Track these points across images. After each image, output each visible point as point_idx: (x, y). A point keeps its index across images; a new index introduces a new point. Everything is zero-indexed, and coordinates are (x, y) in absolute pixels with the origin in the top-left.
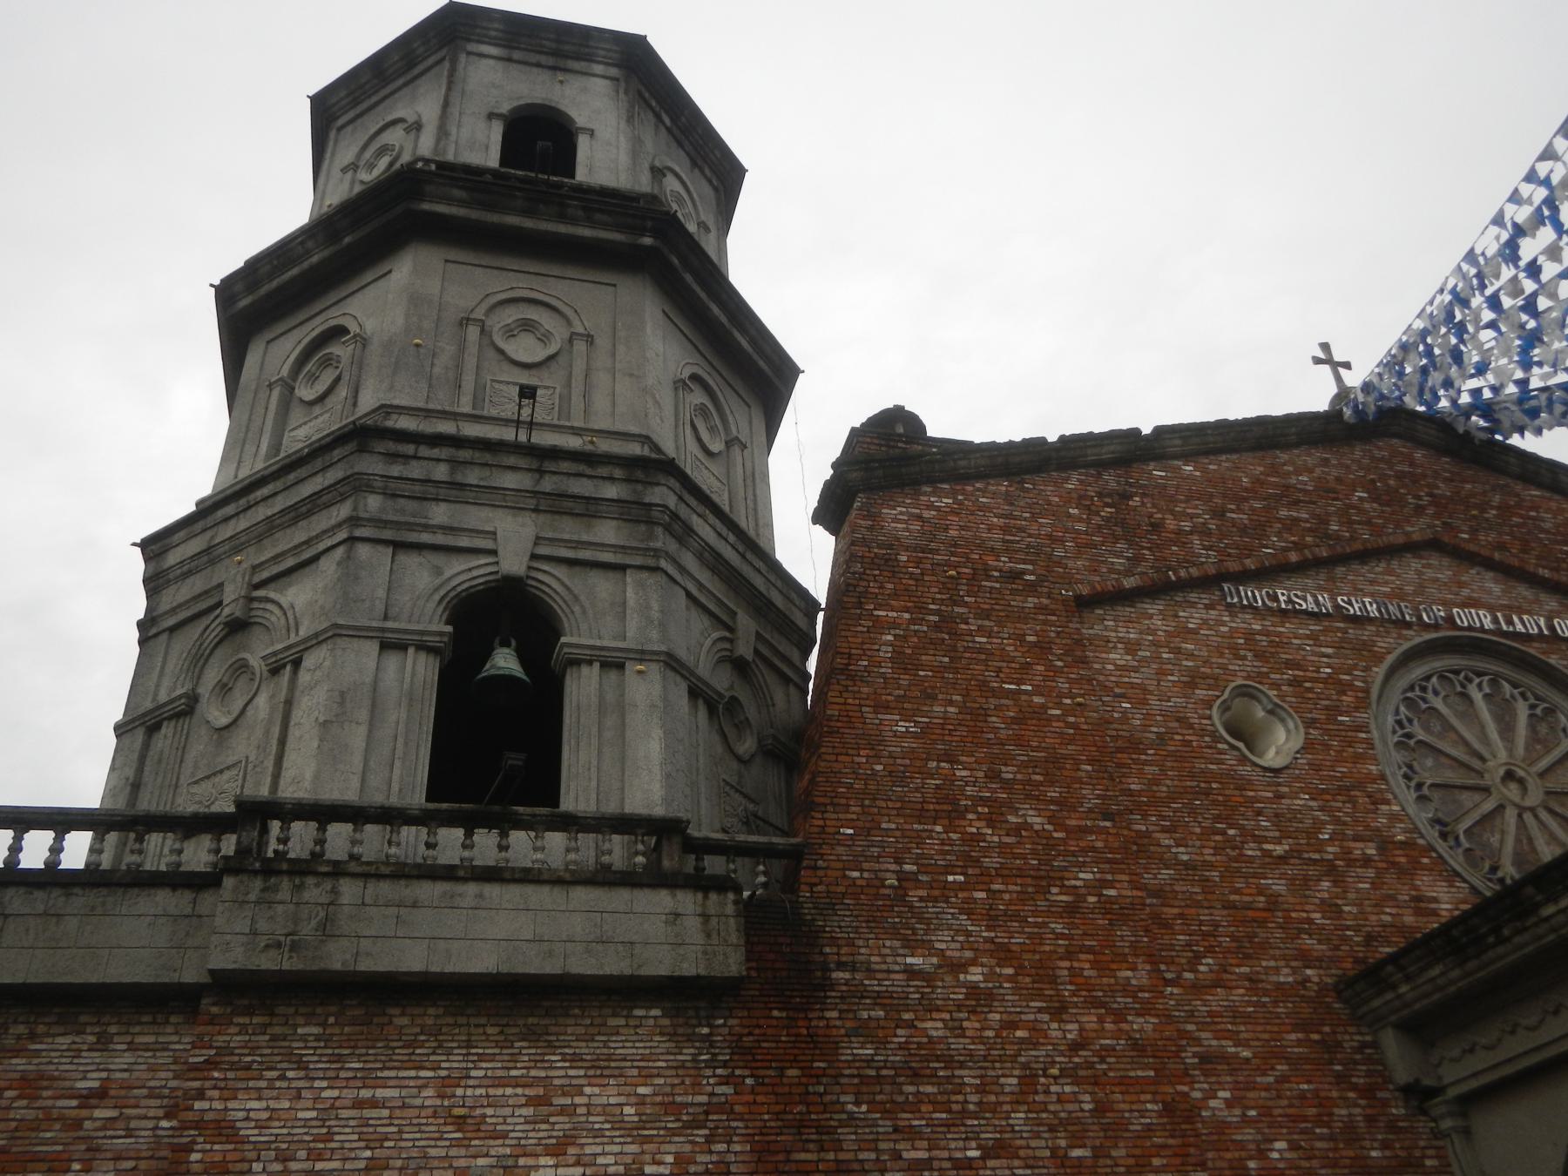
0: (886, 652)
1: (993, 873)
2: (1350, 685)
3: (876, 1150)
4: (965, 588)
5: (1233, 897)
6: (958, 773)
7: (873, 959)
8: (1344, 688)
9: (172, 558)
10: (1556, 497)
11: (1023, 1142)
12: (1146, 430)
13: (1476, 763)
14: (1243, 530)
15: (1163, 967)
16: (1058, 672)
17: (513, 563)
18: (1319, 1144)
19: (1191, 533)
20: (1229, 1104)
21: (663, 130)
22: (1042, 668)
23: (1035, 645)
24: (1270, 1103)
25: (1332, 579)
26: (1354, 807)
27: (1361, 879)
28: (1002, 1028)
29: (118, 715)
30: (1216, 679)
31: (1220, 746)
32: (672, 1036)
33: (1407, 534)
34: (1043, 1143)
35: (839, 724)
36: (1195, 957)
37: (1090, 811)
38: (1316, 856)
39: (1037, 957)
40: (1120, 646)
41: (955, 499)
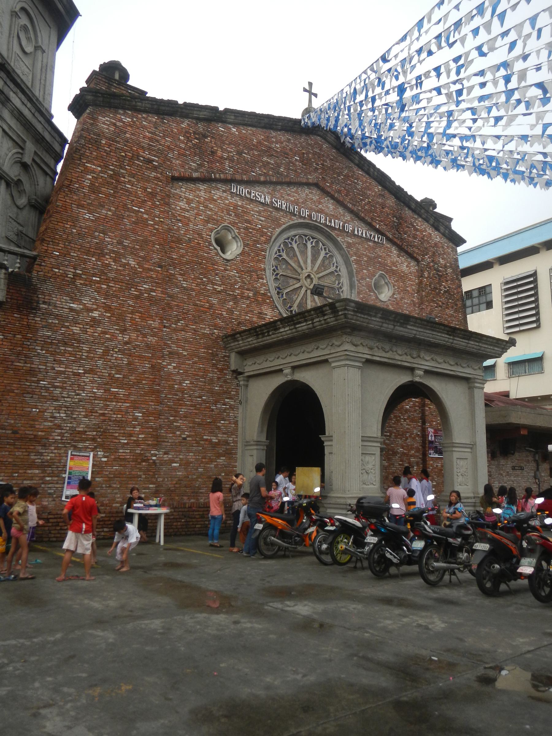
0: (87, 183)
1: (111, 279)
2: (266, 233)
3: (46, 366)
4: (127, 162)
5: (197, 302)
6: (106, 239)
7: (58, 302)
8: (263, 234)
10: (367, 176)
11: (100, 370)
12: (221, 109)
13: (299, 270)
14: (247, 163)
15: (165, 321)
16: (157, 206)
18: (200, 383)
19: (226, 159)
22: (150, 203)
23: (150, 193)
24: (188, 369)
25: (274, 190)
26: (251, 278)
27: (244, 303)
28: (101, 333)
30: (218, 221)
31: (211, 247)
33: (308, 179)
34: (106, 371)
35: (61, 210)
36: (178, 320)
37: (154, 263)
38: (232, 293)
39: (120, 311)
40: (185, 200)
41: (132, 119)
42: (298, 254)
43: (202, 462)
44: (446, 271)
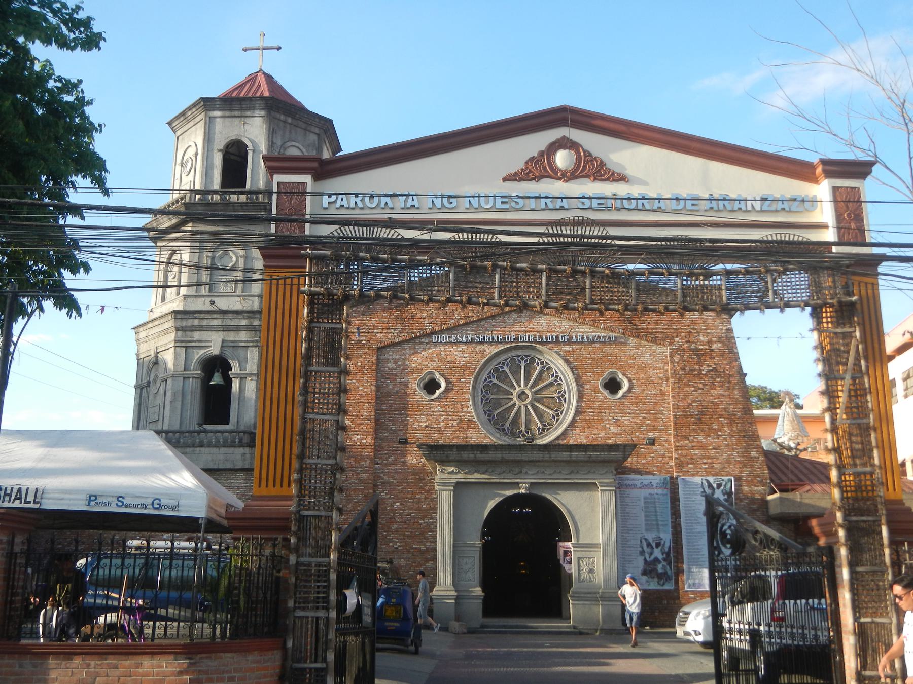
9: (143, 335)
17: (215, 350)
20: (386, 494)
21: (288, 126)
29: (134, 383)
32: (245, 480)
42: (510, 375)
43: (412, 566)
44: (711, 347)
